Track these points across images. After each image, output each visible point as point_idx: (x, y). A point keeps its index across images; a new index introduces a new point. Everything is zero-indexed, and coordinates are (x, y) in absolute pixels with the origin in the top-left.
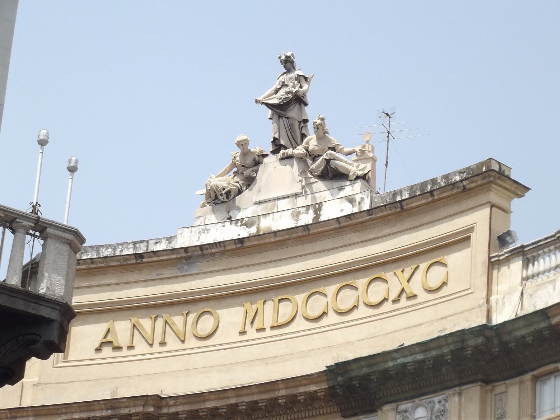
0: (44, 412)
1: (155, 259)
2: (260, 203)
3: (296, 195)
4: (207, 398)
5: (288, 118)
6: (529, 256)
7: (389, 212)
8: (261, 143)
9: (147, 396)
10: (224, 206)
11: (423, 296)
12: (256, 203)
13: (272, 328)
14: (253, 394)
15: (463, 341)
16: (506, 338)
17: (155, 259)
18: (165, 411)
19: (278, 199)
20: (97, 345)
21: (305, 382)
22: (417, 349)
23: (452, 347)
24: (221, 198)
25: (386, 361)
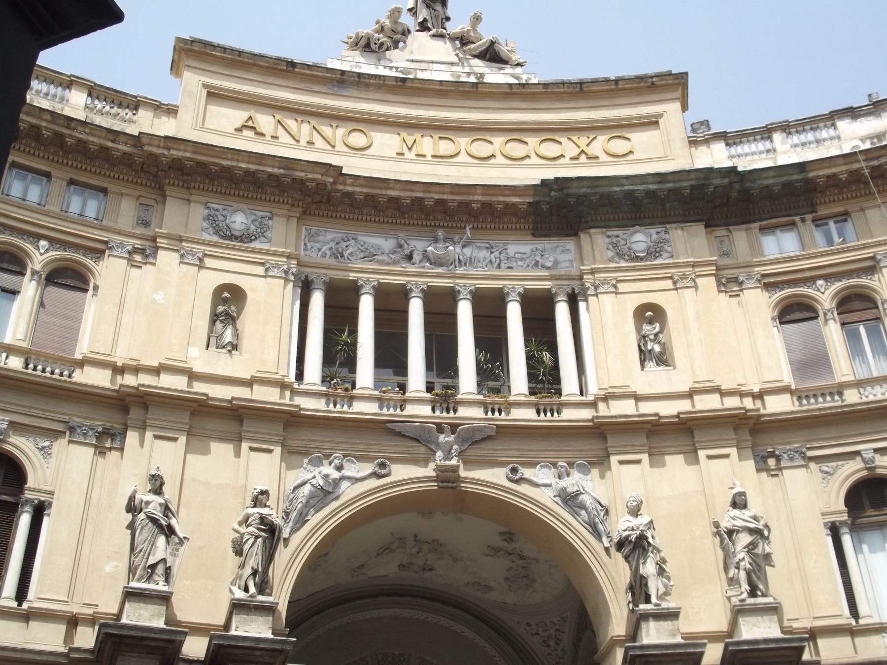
0: (205, 152)
1: (307, 72)
2: (413, 61)
3: (452, 64)
4: (391, 185)
5: (435, 10)
6: (731, 141)
7: (566, 89)
8: (407, 20)
9: (330, 165)
10: (374, 55)
11: (604, 158)
12: (408, 60)
13: (433, 156)
14: (443, 193)
15: (706, 179)
16: (748, 184)
17: (307, 72)
18: (341, 187)
19: (432, 62)
20: (239, 125)
21: (507, 192)
22: (651, 179)
23: (693, 183)
24: (373, 46)
25: (612, 186)
